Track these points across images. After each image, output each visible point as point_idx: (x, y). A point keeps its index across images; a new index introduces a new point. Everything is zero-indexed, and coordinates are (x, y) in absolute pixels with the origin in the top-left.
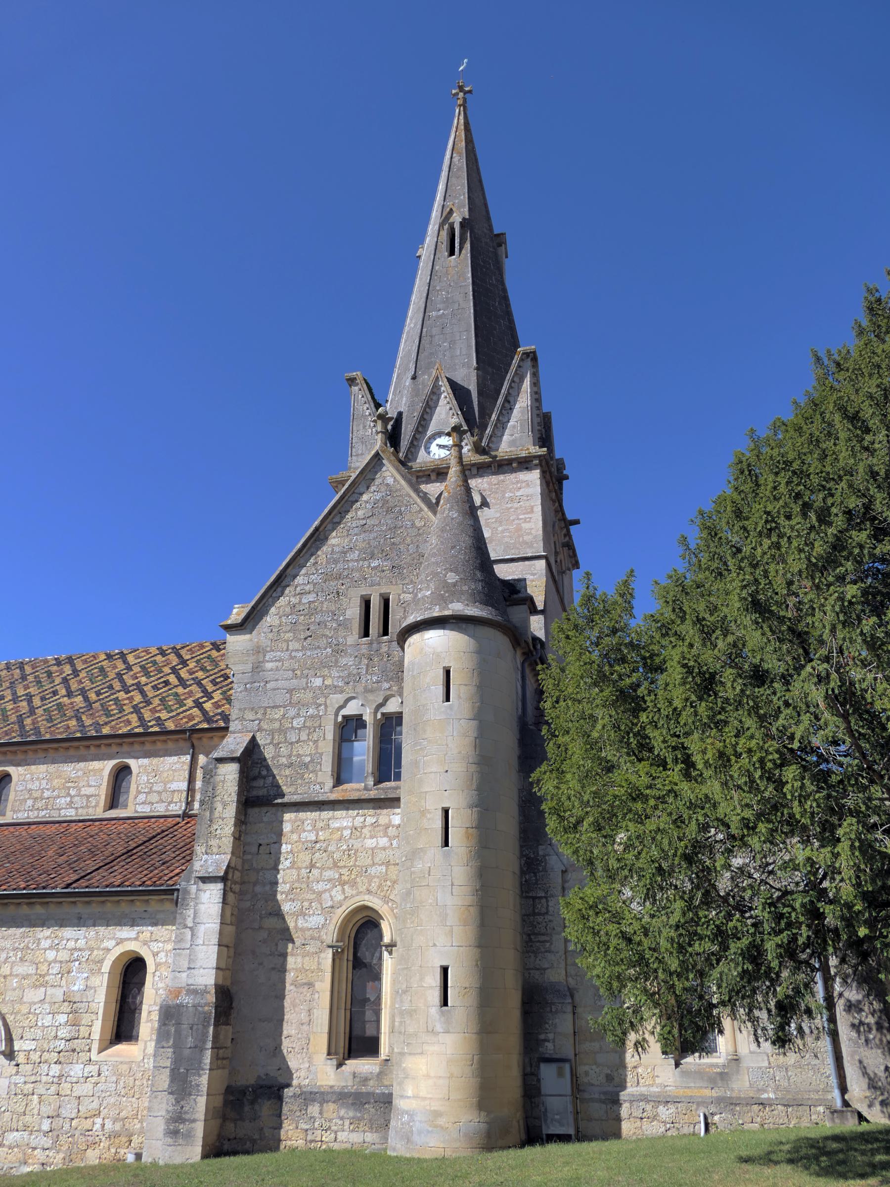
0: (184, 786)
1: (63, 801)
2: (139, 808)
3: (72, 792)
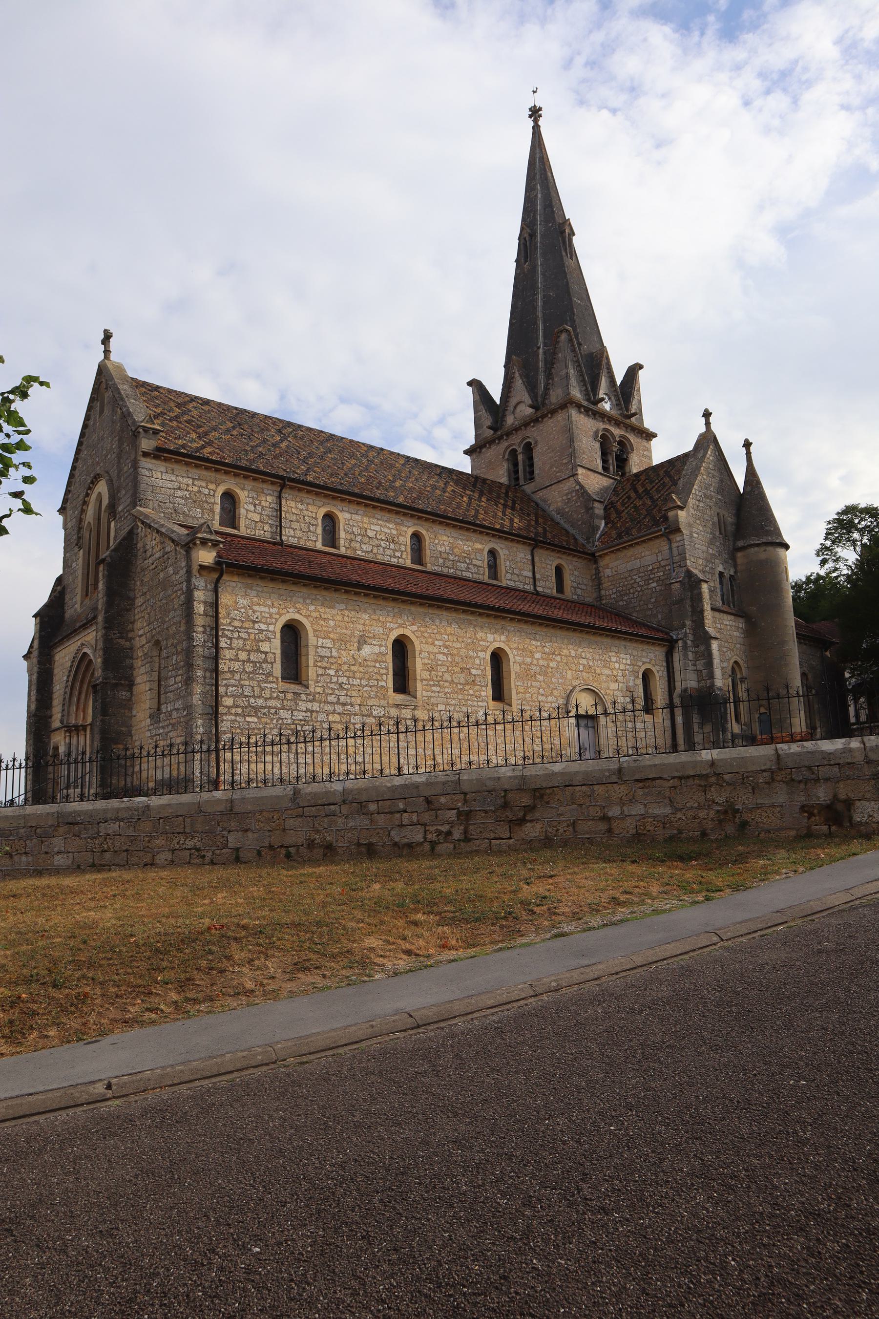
0: (530, 574)
1: (463, 566)
2: (509, 583)
3: (468, 561)
